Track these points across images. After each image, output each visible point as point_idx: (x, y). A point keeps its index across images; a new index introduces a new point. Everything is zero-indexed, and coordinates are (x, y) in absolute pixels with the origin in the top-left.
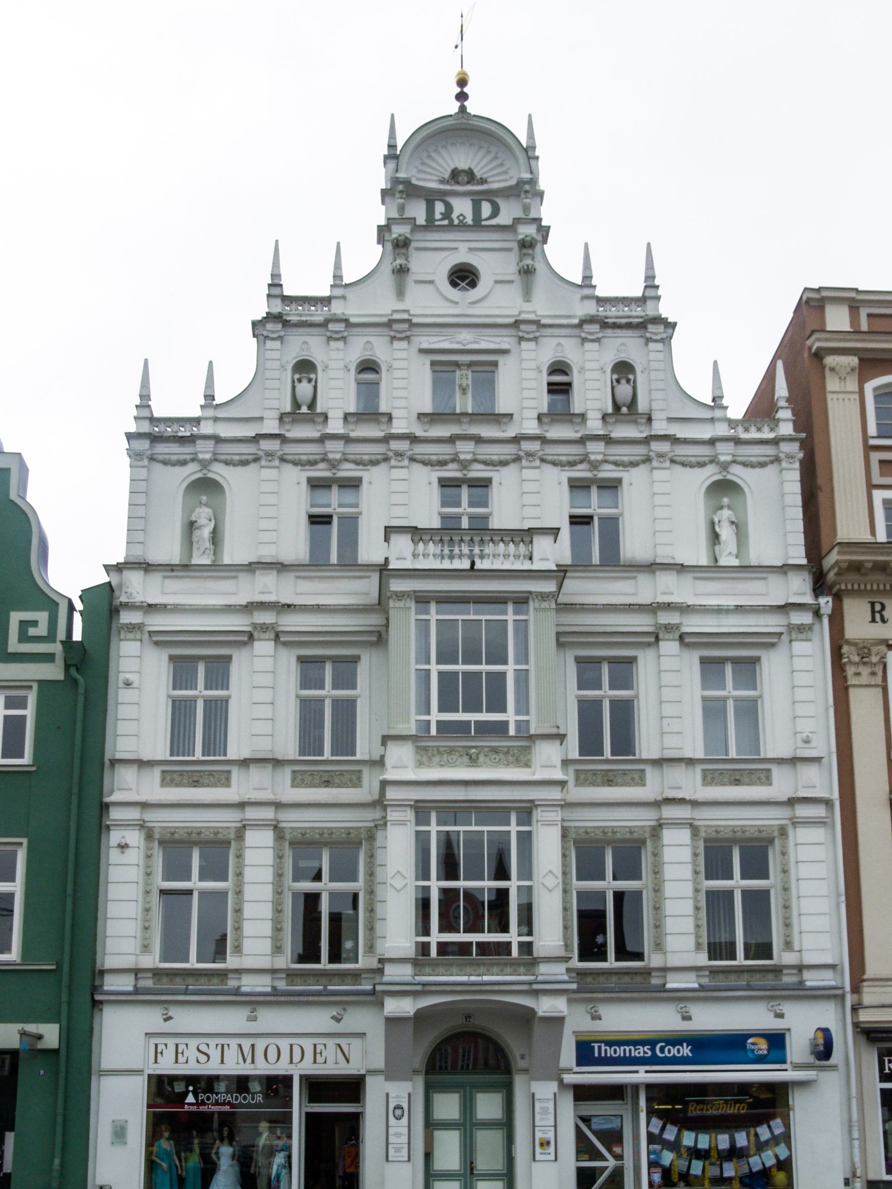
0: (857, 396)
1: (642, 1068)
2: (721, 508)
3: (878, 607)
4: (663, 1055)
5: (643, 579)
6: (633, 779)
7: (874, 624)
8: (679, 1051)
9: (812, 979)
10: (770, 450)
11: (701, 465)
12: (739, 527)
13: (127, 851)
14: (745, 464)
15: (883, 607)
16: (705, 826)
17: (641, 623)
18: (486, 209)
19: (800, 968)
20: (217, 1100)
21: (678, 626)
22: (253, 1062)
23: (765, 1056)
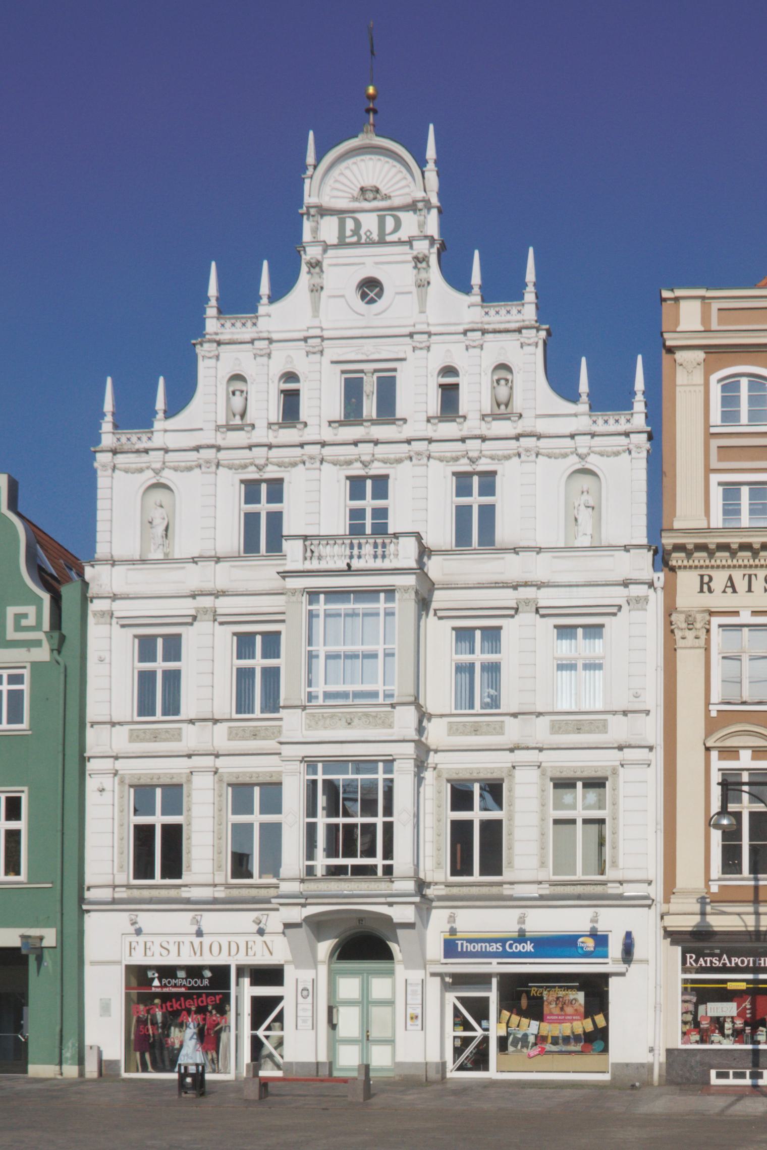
0: (702, 388)
1: (495, 961)
3: (706, 579)
4: (512, 951)
6: (495, 729)
7: (702, 594)
8: (523, 947)
10: (623, 440)
13: (104, 793)
14: (601, 454)
15: (711, 579)
16: (551, 767)
17: (507, 597)
18: (390, 223)
20: (175, 984)
21: (535, 600)
22: (201, 955)
23: (592, 952)
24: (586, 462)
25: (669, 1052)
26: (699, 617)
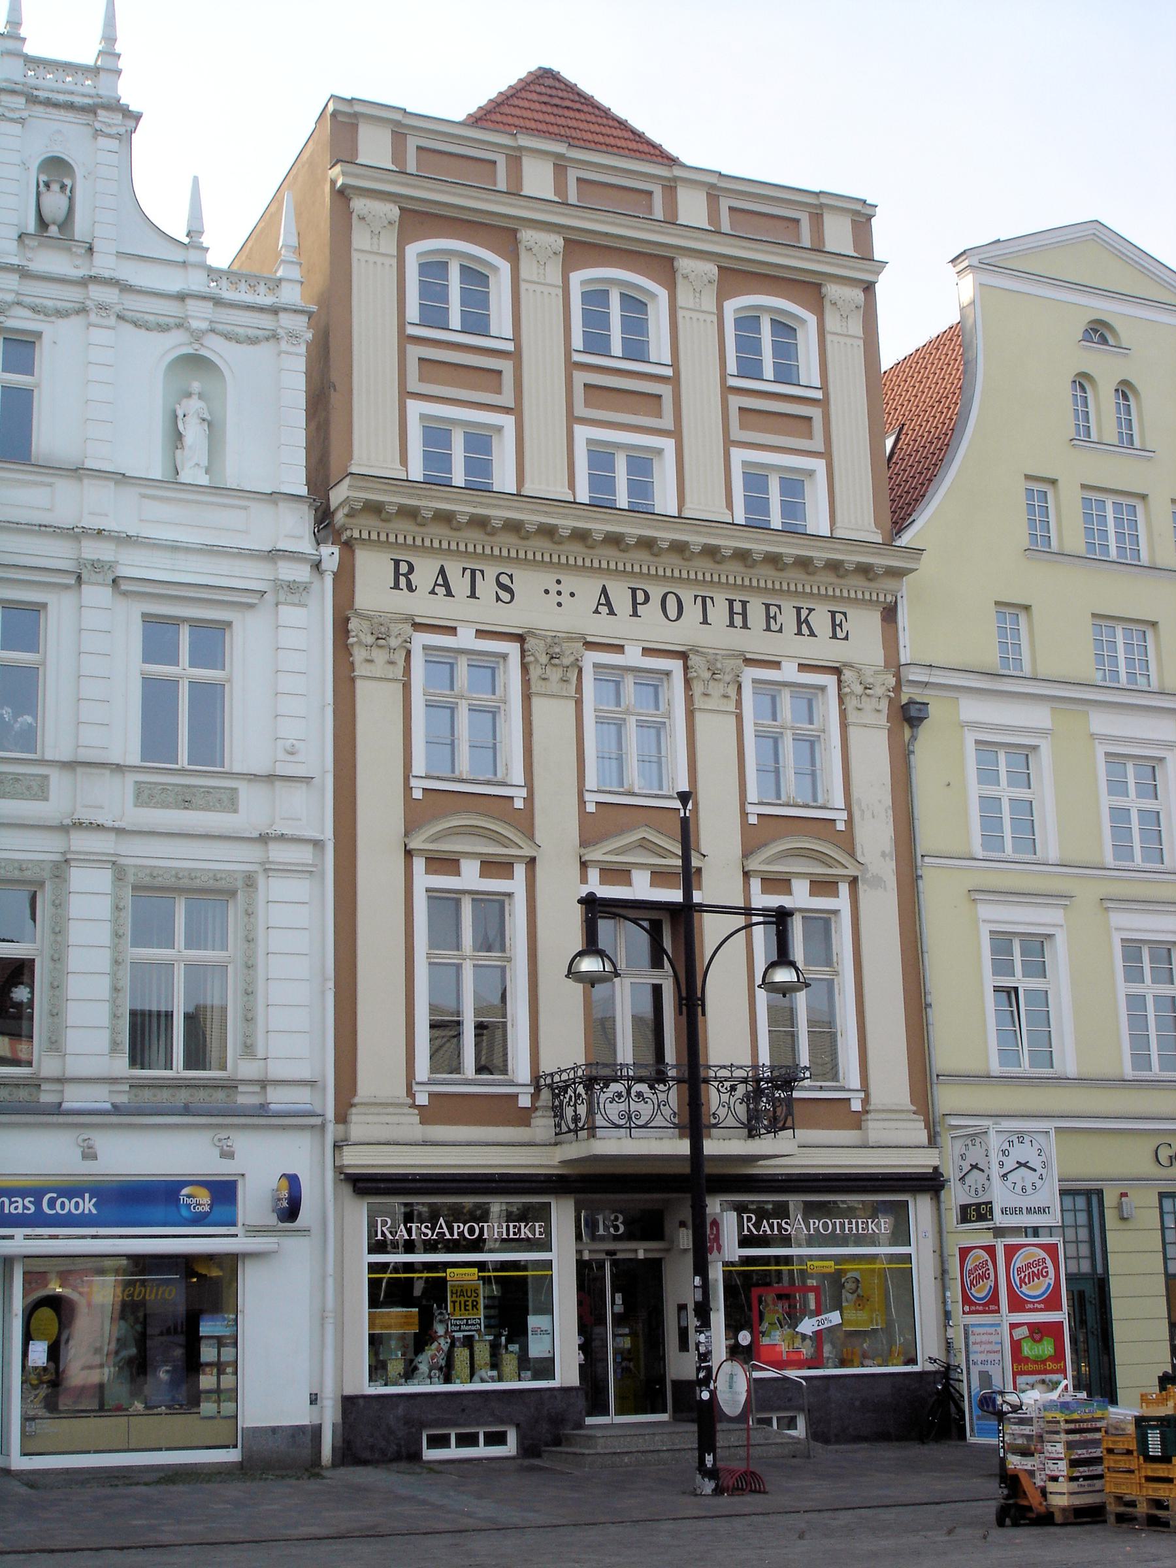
0: (394, 262)
1: (19, 1232)
2: (189, 395)
3: (404, 568)
4: (54, 1212)
5: (65, 488)
6: (29, 788)
8: (77, 1205)
9: (278, 1098)
10: (266, 321)
11: (163, 328)
12: (213, 427)
14: (227, 337)
15: (411, 569)
16: (135, 866)
17: (57, 553)
19: (263, 1084)
21: (111, 566)
23: (207, 1214)
24: (202, 345)
25: (349, 1403)
26: (395, 628)
